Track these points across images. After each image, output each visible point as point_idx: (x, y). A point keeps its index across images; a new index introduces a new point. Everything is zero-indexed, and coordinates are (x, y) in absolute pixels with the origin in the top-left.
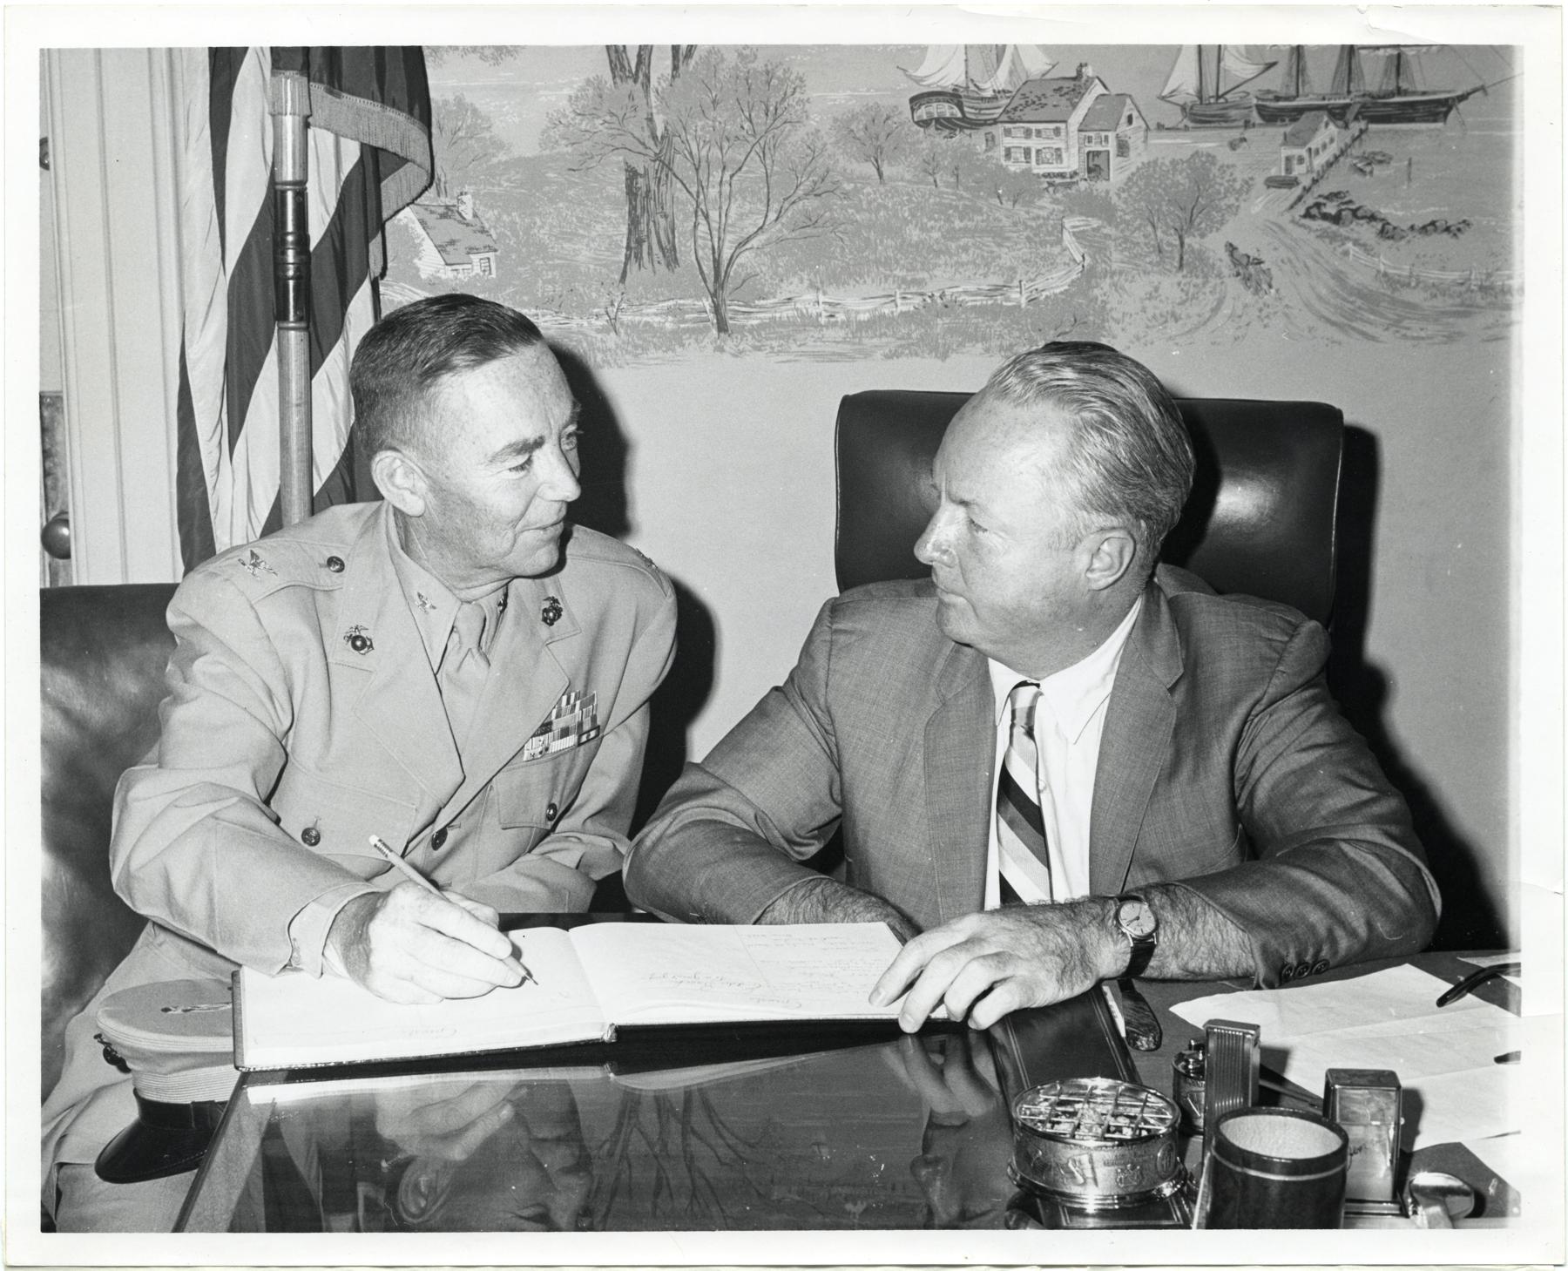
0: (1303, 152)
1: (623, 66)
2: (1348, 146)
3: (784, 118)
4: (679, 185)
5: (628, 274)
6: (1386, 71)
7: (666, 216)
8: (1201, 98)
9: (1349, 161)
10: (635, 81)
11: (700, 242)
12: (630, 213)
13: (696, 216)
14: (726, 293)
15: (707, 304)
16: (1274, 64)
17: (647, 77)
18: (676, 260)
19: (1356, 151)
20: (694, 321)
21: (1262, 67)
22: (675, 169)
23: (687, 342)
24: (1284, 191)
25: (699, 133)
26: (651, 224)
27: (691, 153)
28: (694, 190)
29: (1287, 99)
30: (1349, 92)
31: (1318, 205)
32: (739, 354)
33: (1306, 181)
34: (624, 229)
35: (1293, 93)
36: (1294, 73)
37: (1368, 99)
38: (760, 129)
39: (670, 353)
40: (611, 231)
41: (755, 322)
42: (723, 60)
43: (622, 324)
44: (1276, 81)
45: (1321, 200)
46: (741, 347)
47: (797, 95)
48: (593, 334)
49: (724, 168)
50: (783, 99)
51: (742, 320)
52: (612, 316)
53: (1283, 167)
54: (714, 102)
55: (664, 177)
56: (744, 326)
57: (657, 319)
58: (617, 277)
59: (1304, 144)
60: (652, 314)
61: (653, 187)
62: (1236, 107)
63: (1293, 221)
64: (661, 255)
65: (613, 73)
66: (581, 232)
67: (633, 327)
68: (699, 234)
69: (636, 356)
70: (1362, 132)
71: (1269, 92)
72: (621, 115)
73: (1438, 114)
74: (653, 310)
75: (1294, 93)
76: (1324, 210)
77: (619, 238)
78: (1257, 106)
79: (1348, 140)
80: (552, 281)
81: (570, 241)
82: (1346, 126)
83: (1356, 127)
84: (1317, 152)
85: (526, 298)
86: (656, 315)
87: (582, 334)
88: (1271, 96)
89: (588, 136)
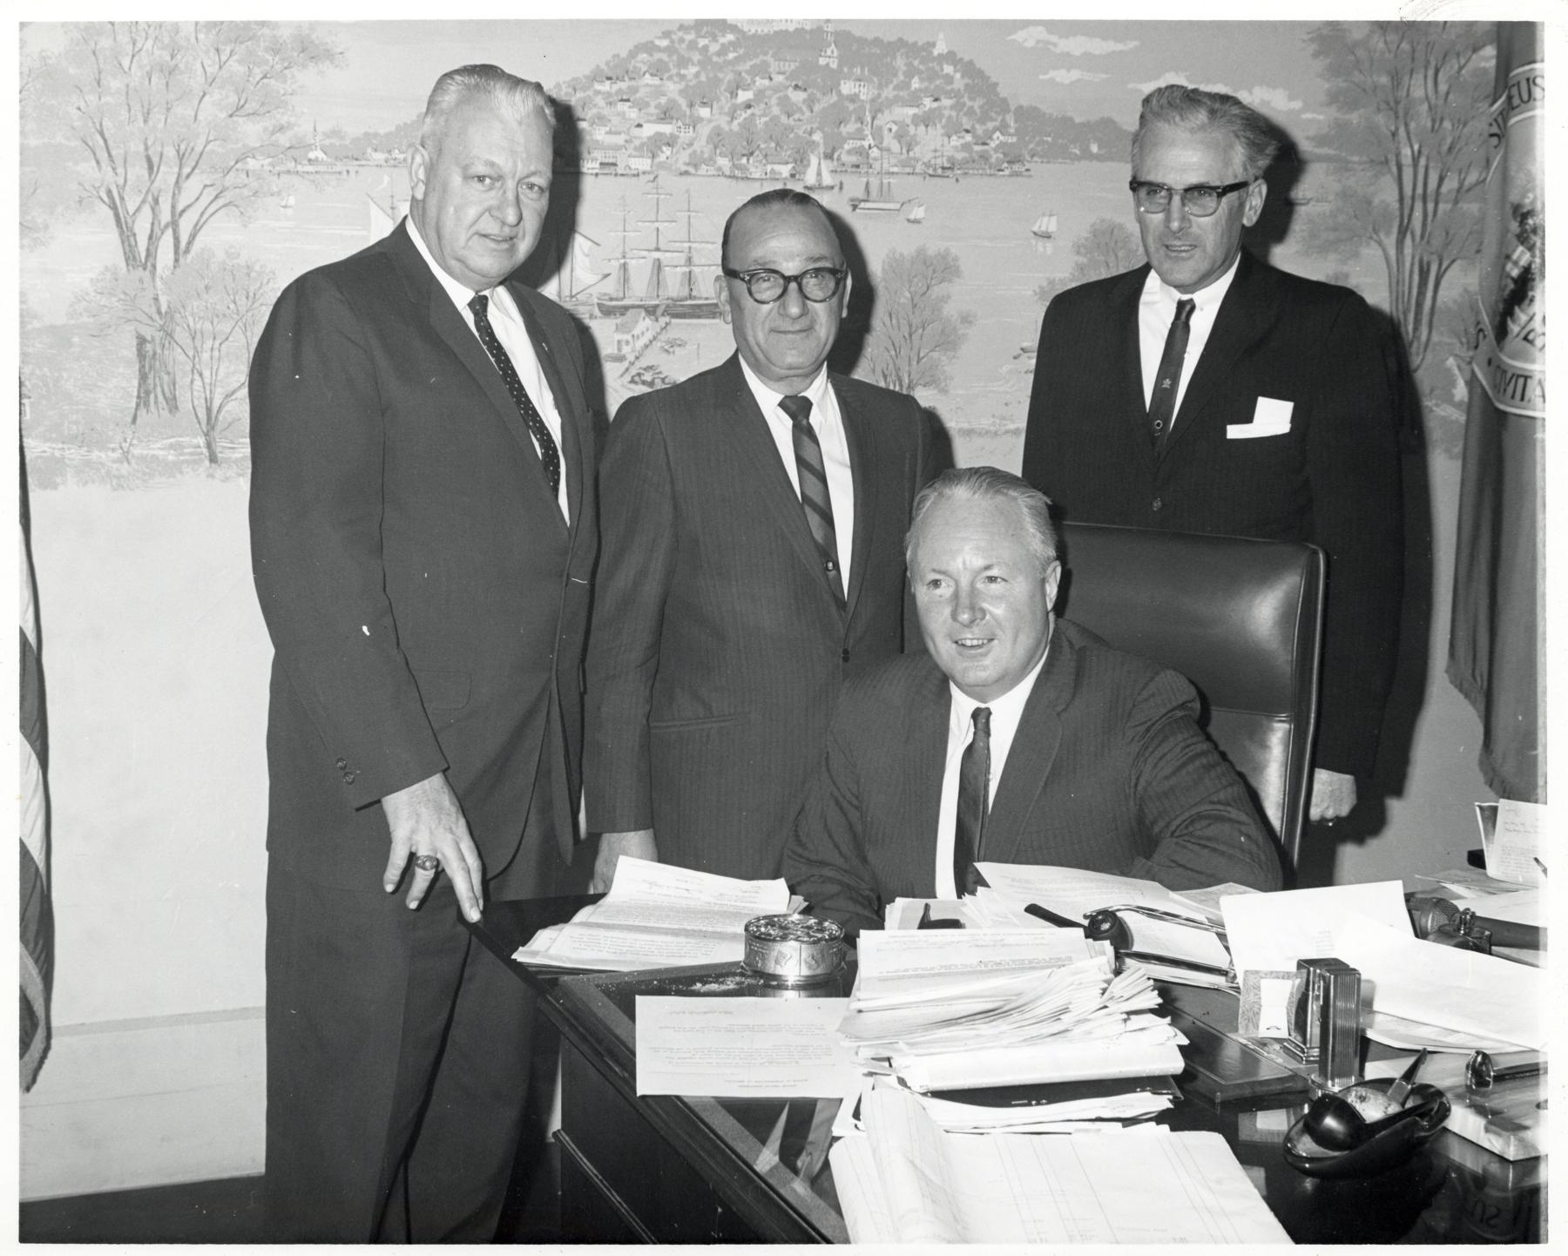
0: (628, 337)
1: (134, 258)
2: (659, 334)
3: (260, 301)
4: (180, 350)
5: (139, 420)
6: (682, 285)
7: (168, 373)
8: (560, 297)
9: (659, 344)
10: (145, 269)
11: (195, 393)
12: (140, 371)
13: (193, 371)
14: (216, 434)
15: (201, 441)
16: (609, 275)
17: (154, 266)
18: (177, 408)
19: (663, 337)
20: (191, 454)
21: (600, 277)
22: (176, 338)
23: (185, 470)
24: (617, 364)
25: (196, 311)
26: (157, 379)
27: (188, 326)
28: (191, 354)
29: (617, 300)
30: (658, 296)
31: (639, 375)
32: (226, 479)
33: (631, 358)
34: (135, 383)
35: (621, 295)
36: (622, 281)
37: (670, 301)
38: (243, 310)
39: (172, 480)
40: (124, 384)
41: (241, 455)
42: (214, 256)
43: (133, 456)
44: (610, 287)
45: (641, 371)
46: (228, 475)
47: (270, 284)
48: (110, 464)
49: (214, 338)
50: (260, 288)
51: (228, 454)
52: (125, 449)
53: (616, 347)
54: (207, 288)
55: (167, 344)
56: (230, 458)
57: (161, 453)
58: (129, 419)
59: (630, 331)
60: (157, 449)
61: (159, 351)
62: (584, 304)
63: (623, 386)
64: (164, 403)
65: (127, 260)
66: (101, 384)
67: (142, 458)
68: (195, 387)
69: (144, 481)
70: (667, 324)
71: (605, 294)
72: (133, 293)
73: (715, 313)
74: (158, 445)
75: (621, 295)
76: (643, 378)
77: (130, 390)
78: (598, 304)
79: (658, 330)
80: (76, 423)
81: (91, 390)
82: (657, 320)
83: (663, 320)
84: (638, 337)
85: (54, 435)
86: (160, 449)
87: (101, 463)
88: (607, 298)
89: (106, 310)
